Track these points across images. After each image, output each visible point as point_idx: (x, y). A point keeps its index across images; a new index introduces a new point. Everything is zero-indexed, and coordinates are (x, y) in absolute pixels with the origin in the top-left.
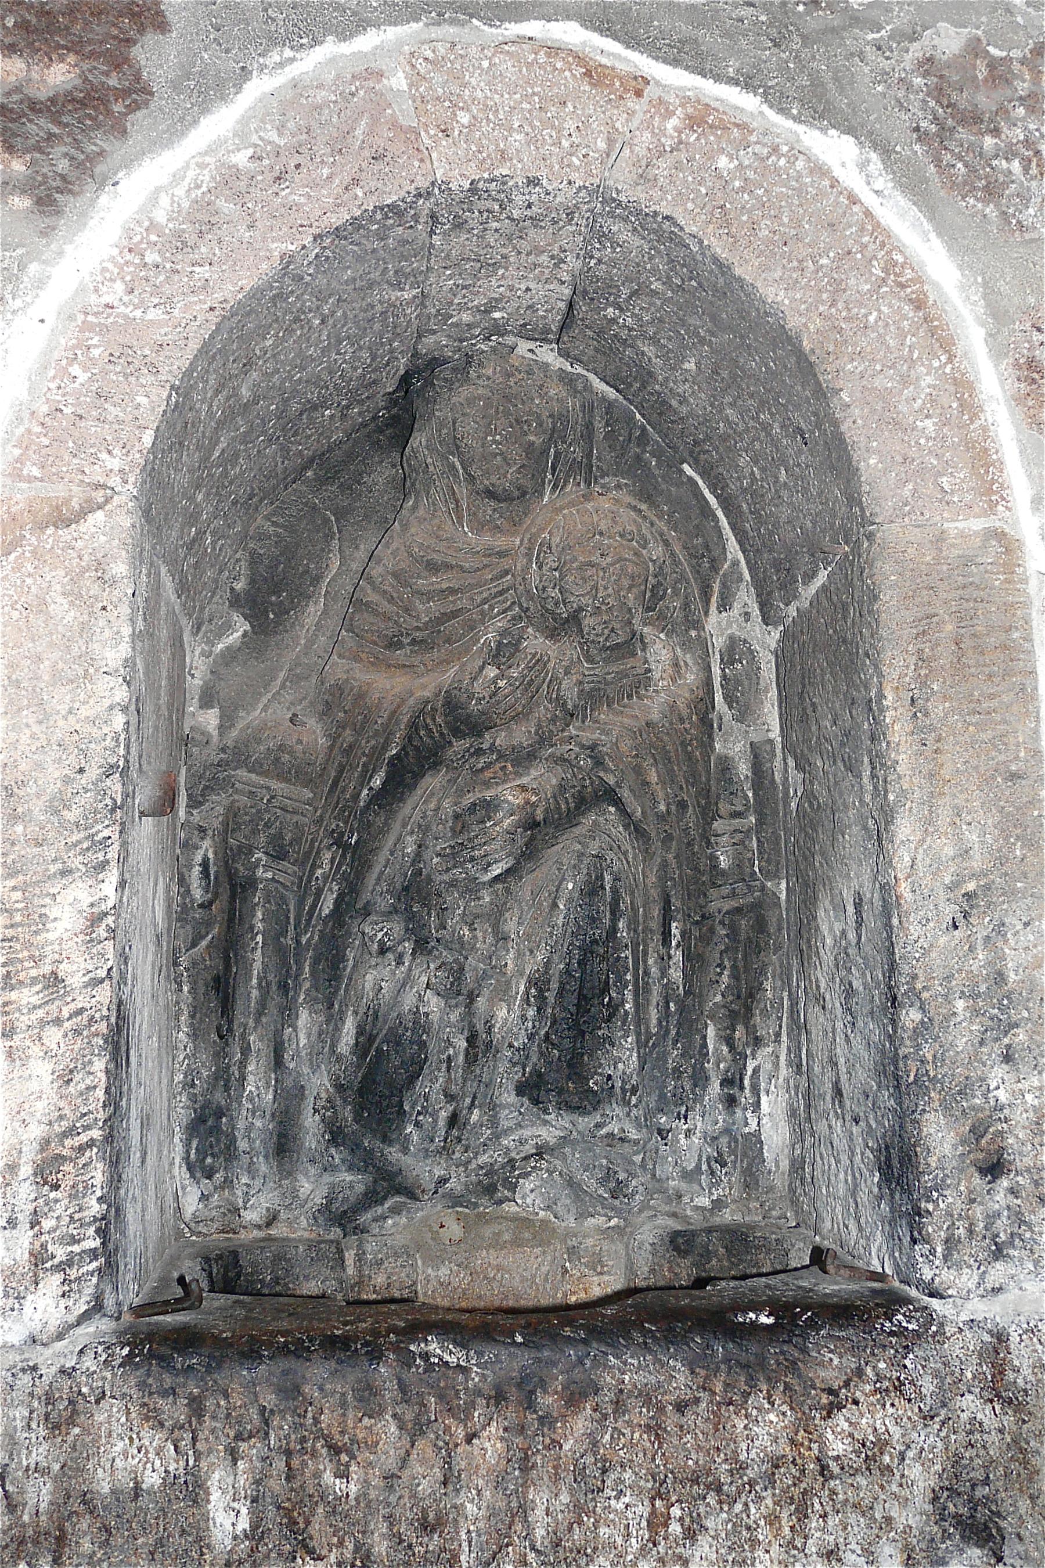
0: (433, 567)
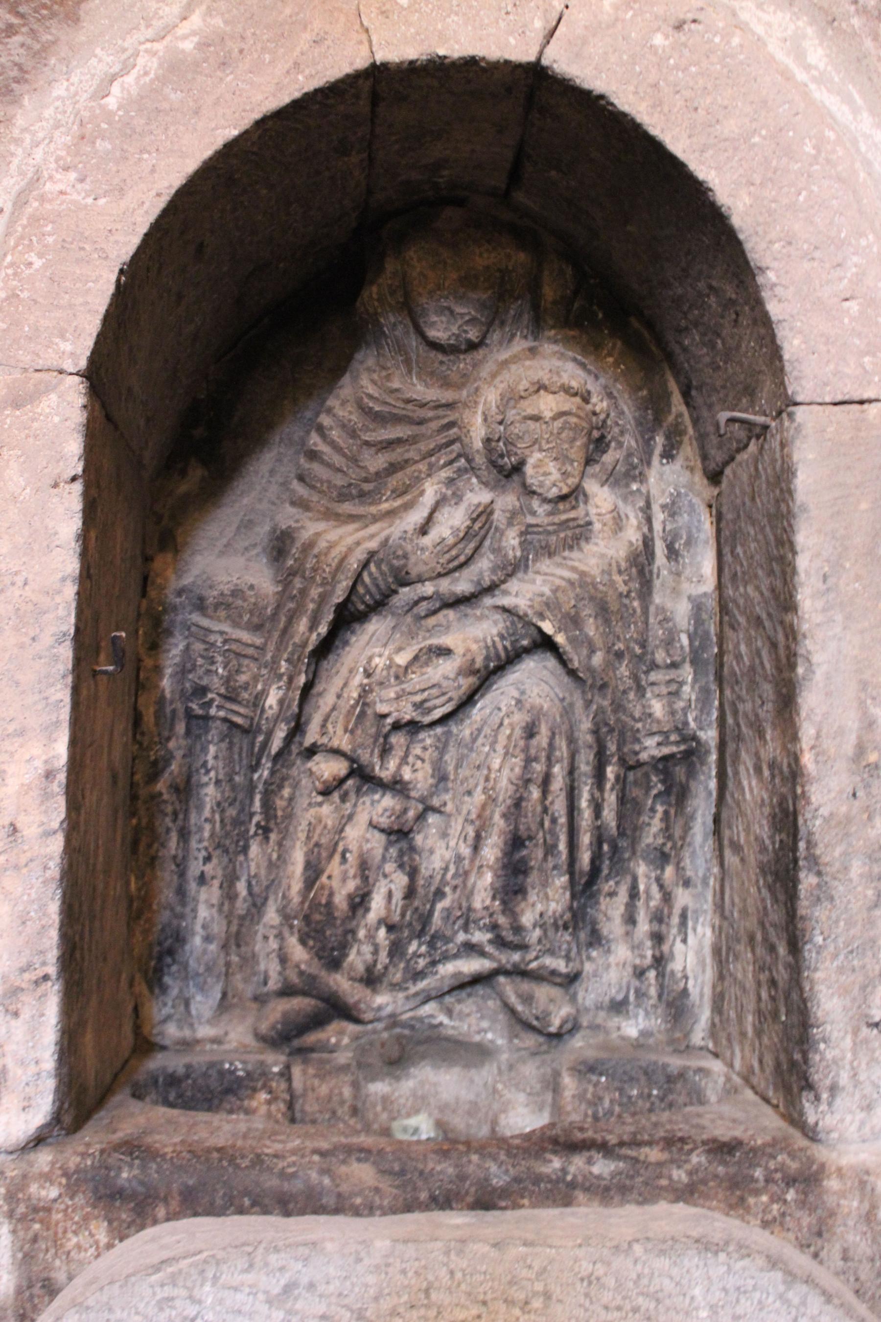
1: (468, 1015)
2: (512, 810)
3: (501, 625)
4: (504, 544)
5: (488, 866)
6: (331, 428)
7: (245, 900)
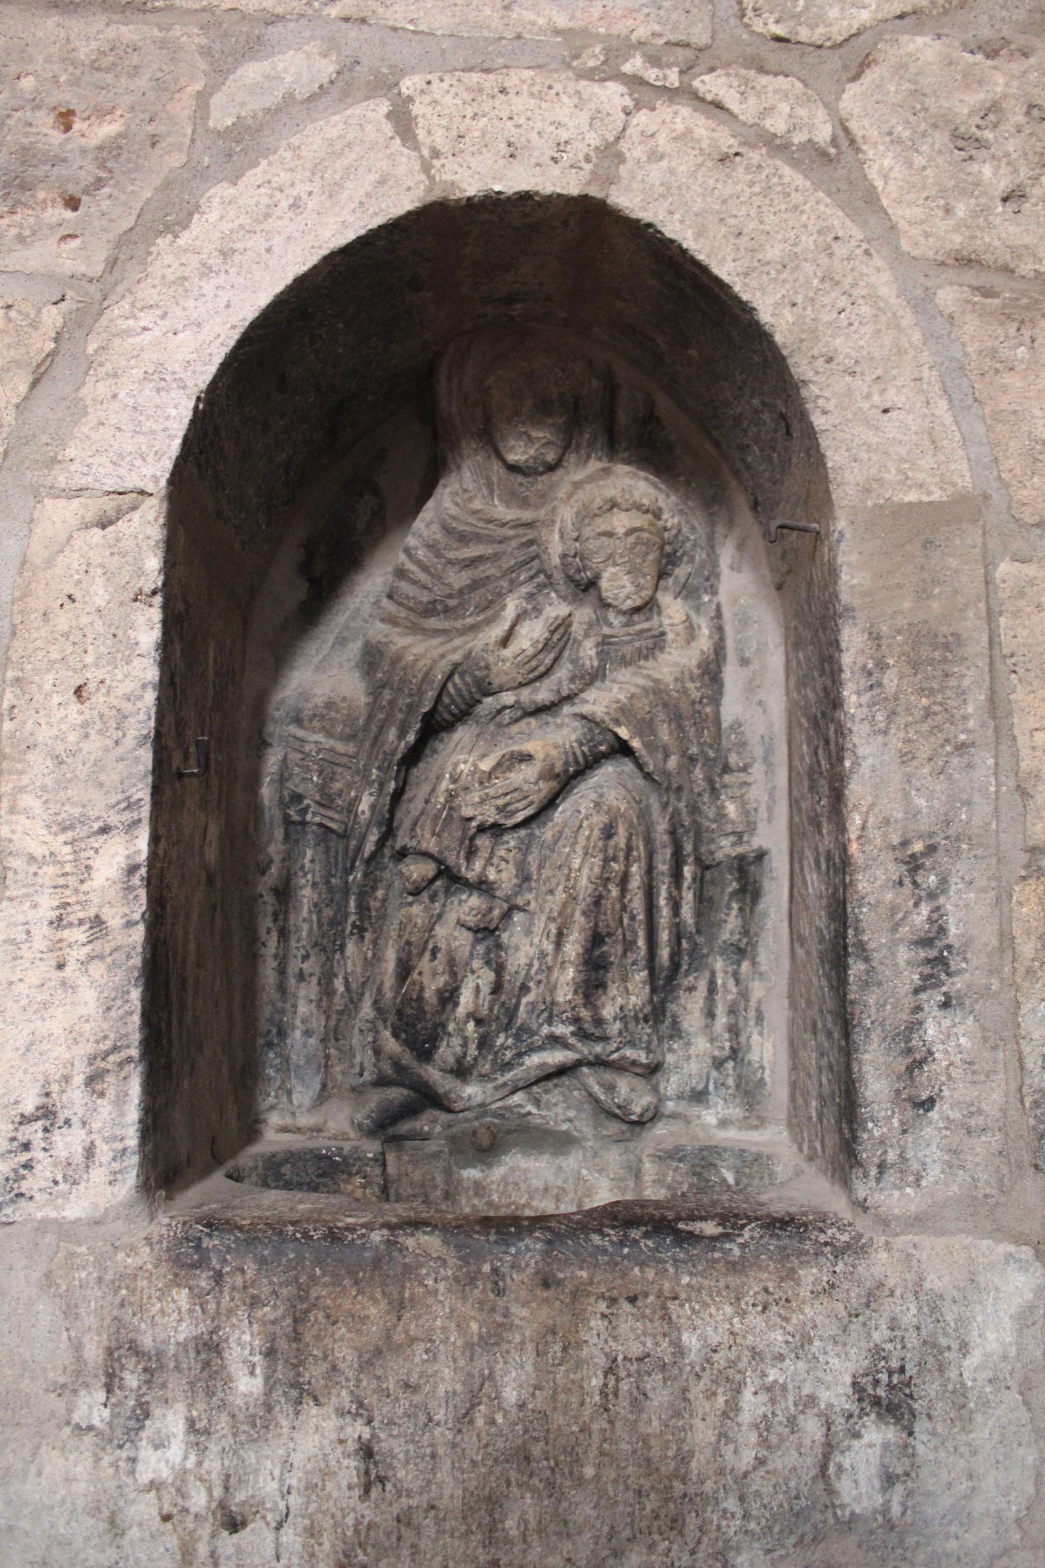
0: (463, 539)
1: (555, 1105)
2: (592, 907)
3: (579, 732)
4: (581, 654)
5: (570, 962)
6: (416, 549)
7: (343, 996)
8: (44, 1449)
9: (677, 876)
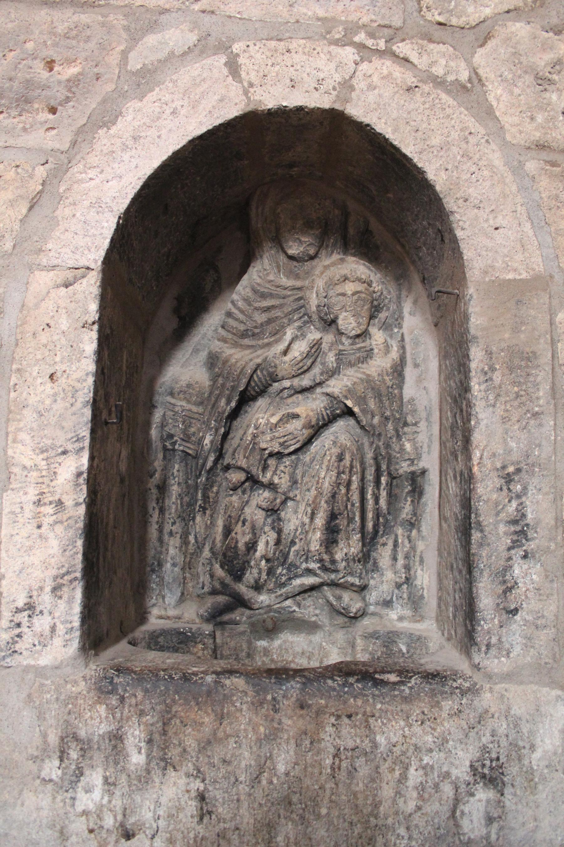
0: (263, 296)
1: (309, 607)
2: (331, 499)
3: (325, 402)
4: (327, 360)
5: (318, 528)
6: (238, 301)
7: (194, 545)
8: (25, 791)
9: (377, 482)
